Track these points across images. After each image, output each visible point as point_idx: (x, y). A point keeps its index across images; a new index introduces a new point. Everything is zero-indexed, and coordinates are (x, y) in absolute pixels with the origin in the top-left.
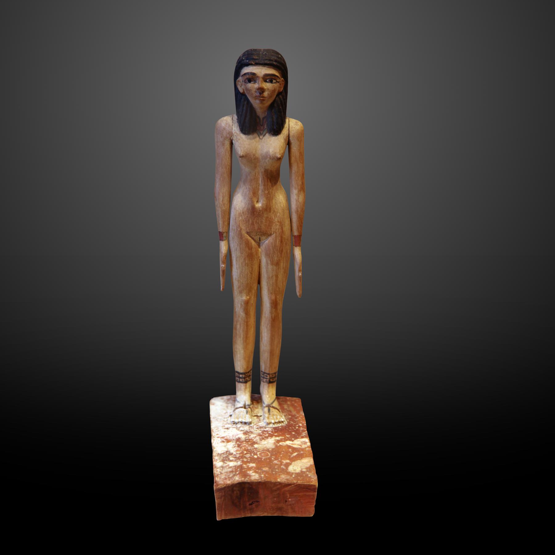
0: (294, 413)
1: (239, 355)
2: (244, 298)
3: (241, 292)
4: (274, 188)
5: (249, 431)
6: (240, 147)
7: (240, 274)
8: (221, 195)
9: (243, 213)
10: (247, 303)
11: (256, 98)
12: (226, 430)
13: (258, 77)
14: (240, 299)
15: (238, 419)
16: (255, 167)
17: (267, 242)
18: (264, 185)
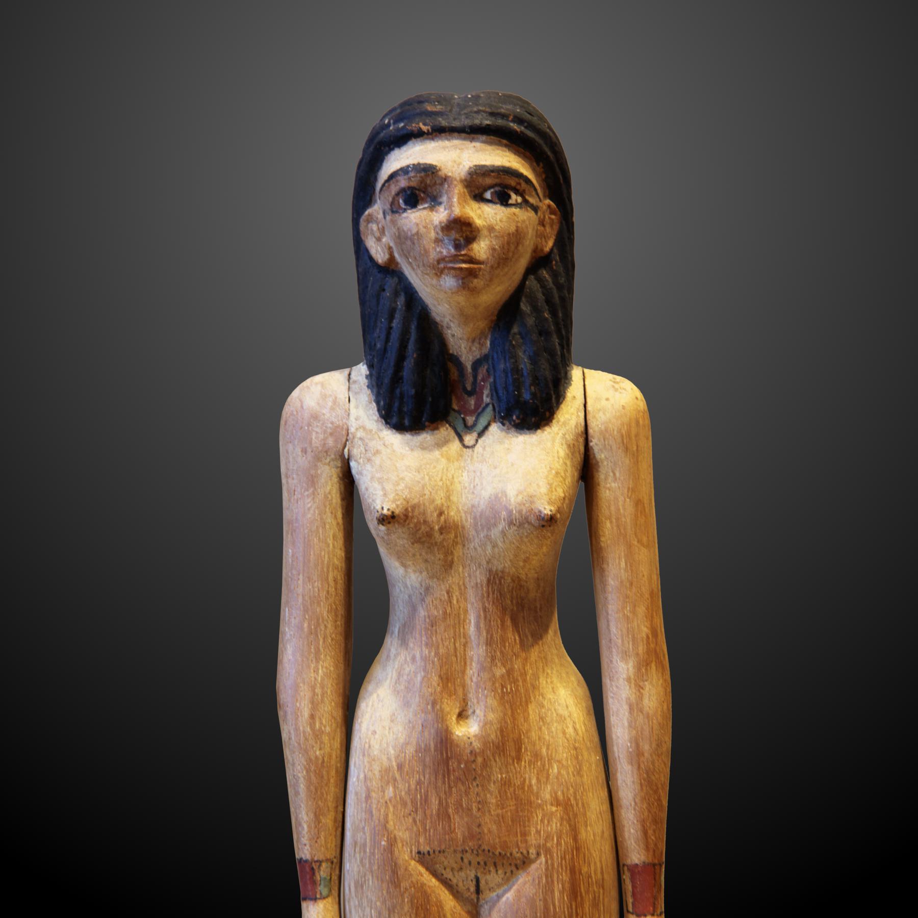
4: (534, 653)
6: (380, 481)
8: (305, 693)
9: (400, 767)
11: (439, 268)
13: (446, 179)
16: (448, 566)
17: (510, 895)
18: (489, 642)
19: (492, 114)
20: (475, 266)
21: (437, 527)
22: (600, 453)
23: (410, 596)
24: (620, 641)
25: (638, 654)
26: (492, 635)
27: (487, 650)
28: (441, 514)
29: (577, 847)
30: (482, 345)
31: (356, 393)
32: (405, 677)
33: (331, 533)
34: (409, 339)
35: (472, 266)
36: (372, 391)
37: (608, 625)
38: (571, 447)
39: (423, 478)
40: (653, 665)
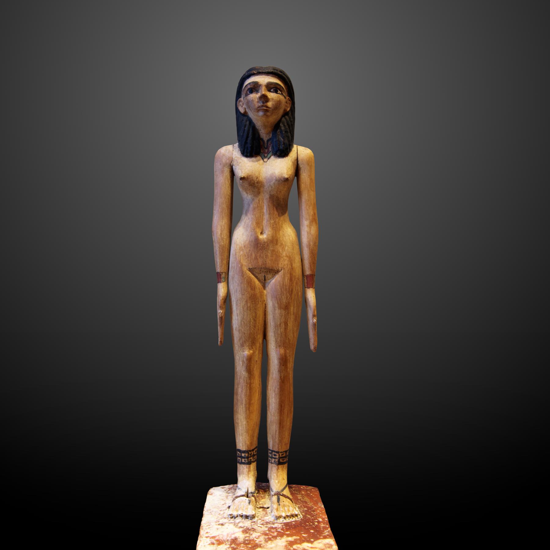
0: (310, 504)
1: (240, 428)
2: (247, 352)
3: (242, 345)
4: (282, 218)
5: (250, 527)
6: (241, 169)
7: (241, 321)
8: (219, 228)
9: (244, 246)
10: (250, 359)
11: (258, 110)
12: (220, 526)
13: (260, 85)
14: (242, 354)
15: (237, 511)
16: (259, 193)
17: (274, 281)
18: (270, 214)
22: (301, 166)
29: (292, 268)
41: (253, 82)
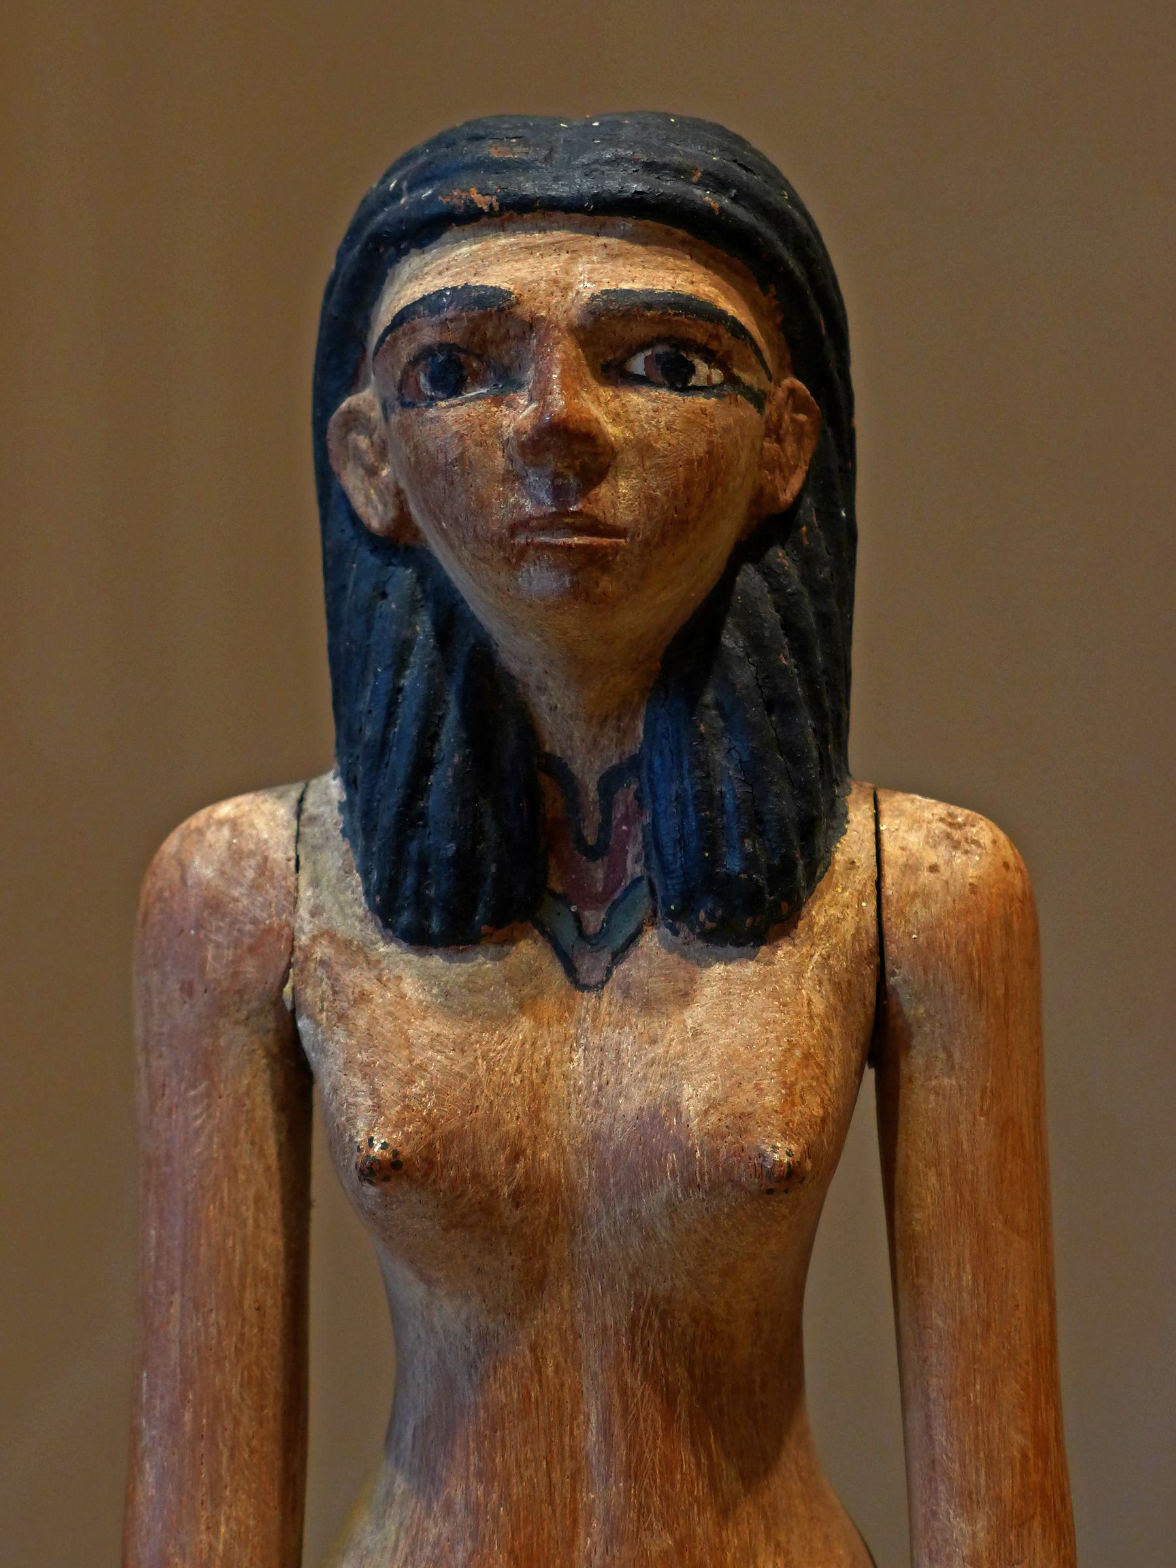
6: (367, 1070)
13: (532, 325)
16: (535, 1284)
18: (633, 1473)
19: (650, 167)
20: (605, 541)
21: (506, 1191)
23: (439, 1353)
24: (957, 1466)
25: (999, 1499)
26: (640, 1455)
27: (627, 1491)
28: (516, 1157)
30: (624, 734)
31: (315, 848)
32: (428, 1551)
33: (251, 1193)
34: (442, 718)
35: (596, 540)
36: (354, 845)
37: (928, 1426)
38: (842, 989)
39: (473, 1067)
40: (1036, 1525)
41: (463, 296)
